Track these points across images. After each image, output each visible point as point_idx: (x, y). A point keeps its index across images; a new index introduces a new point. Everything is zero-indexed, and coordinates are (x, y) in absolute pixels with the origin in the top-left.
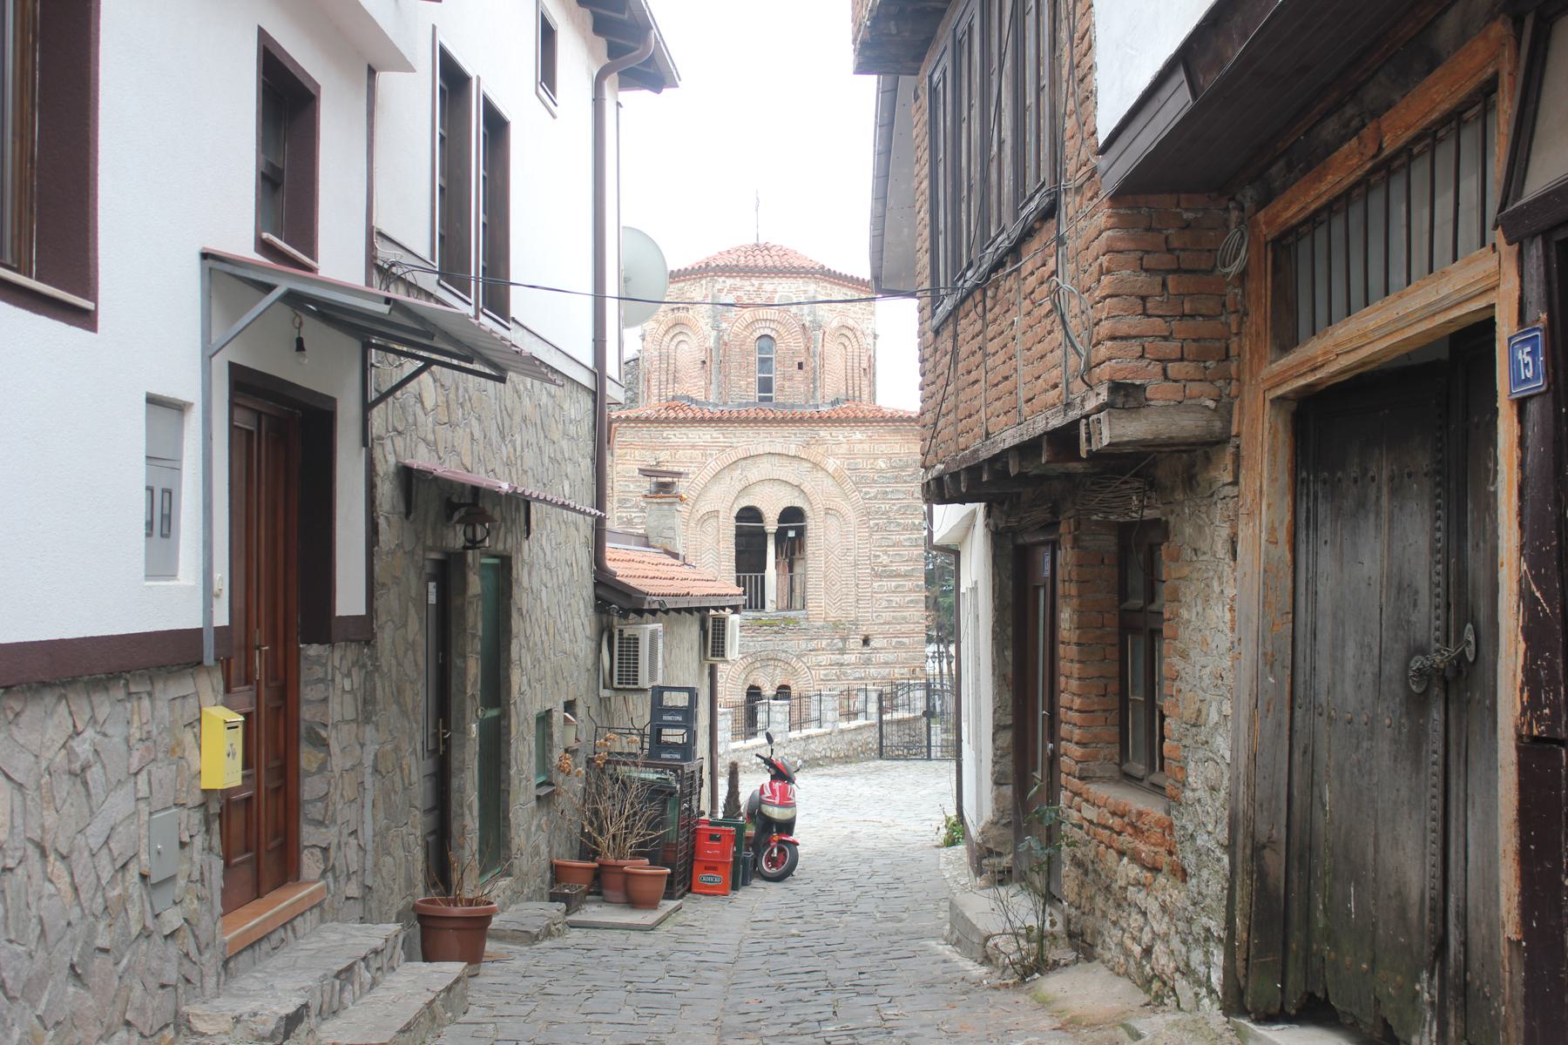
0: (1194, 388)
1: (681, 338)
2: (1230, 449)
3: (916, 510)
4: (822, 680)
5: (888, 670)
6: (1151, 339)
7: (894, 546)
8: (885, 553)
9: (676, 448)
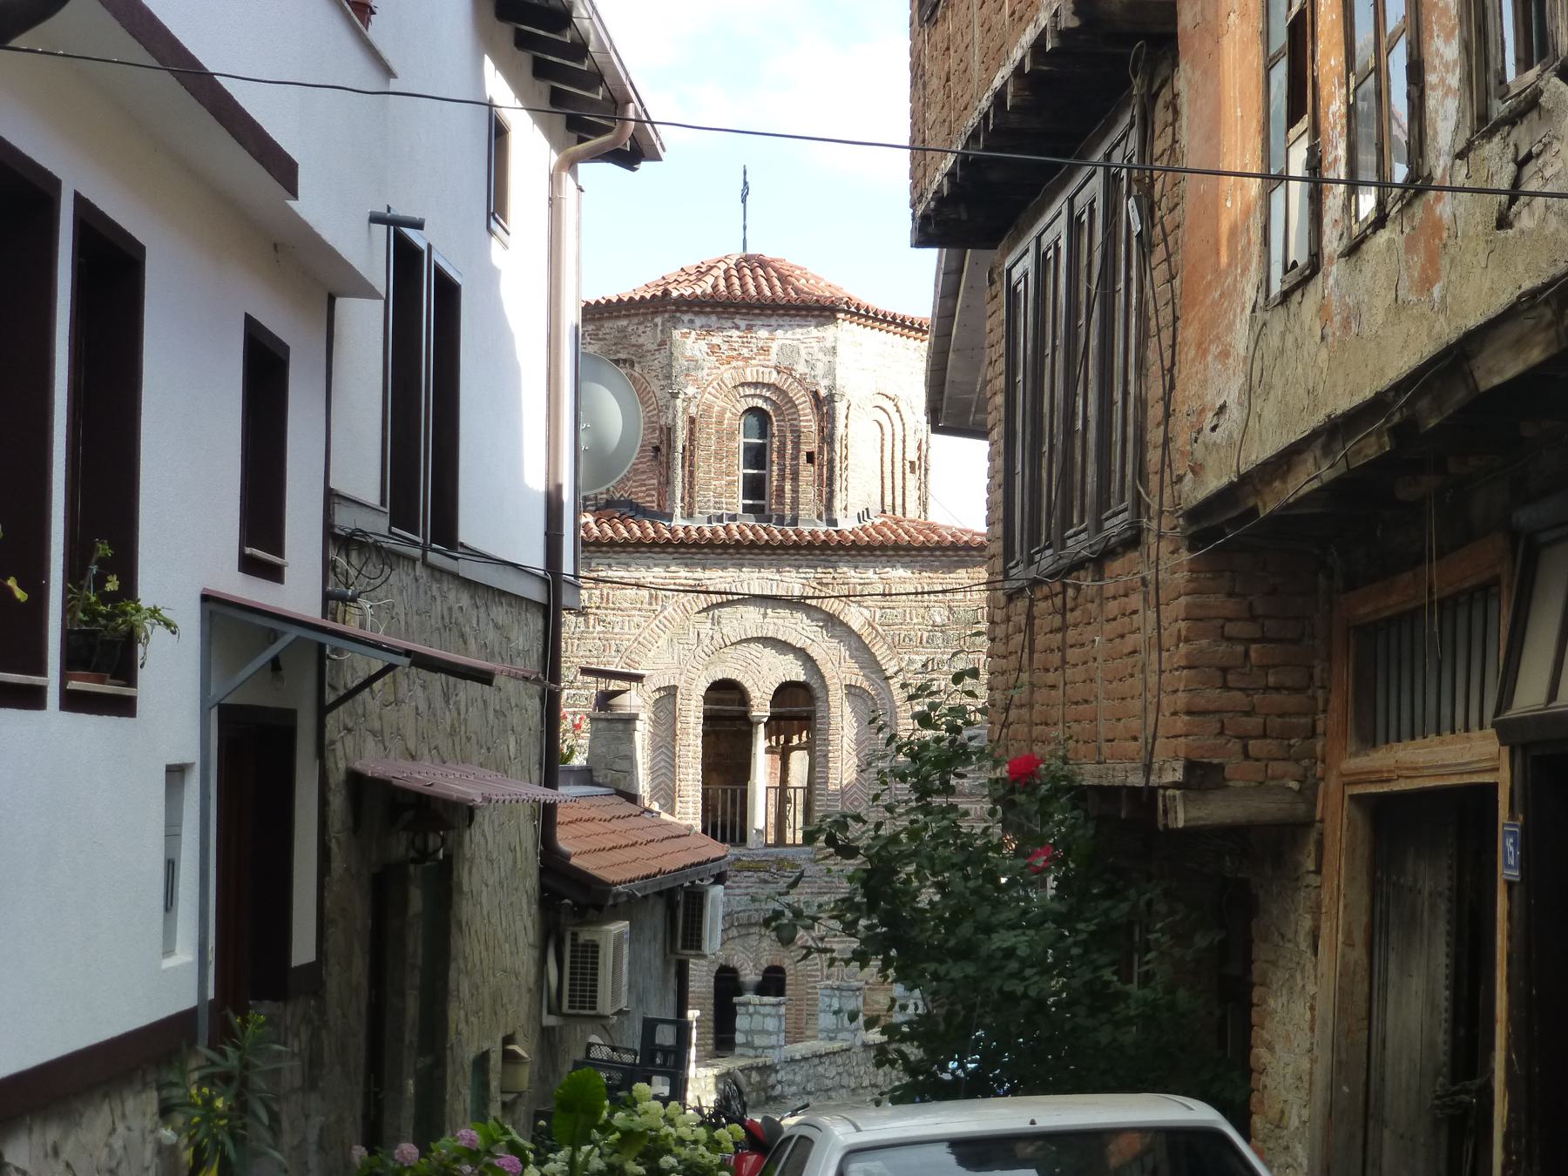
0: (1277, 768)
2: (1314, 836)
6: (1231, 715)
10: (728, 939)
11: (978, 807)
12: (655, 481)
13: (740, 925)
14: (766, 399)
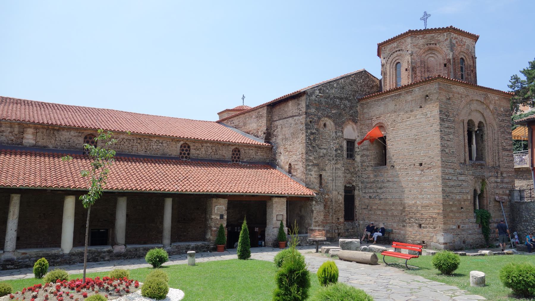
1: (431, 55)
5: (507, 185)
7: (506, 140)
12: (446, 72)
14: (464, 56)
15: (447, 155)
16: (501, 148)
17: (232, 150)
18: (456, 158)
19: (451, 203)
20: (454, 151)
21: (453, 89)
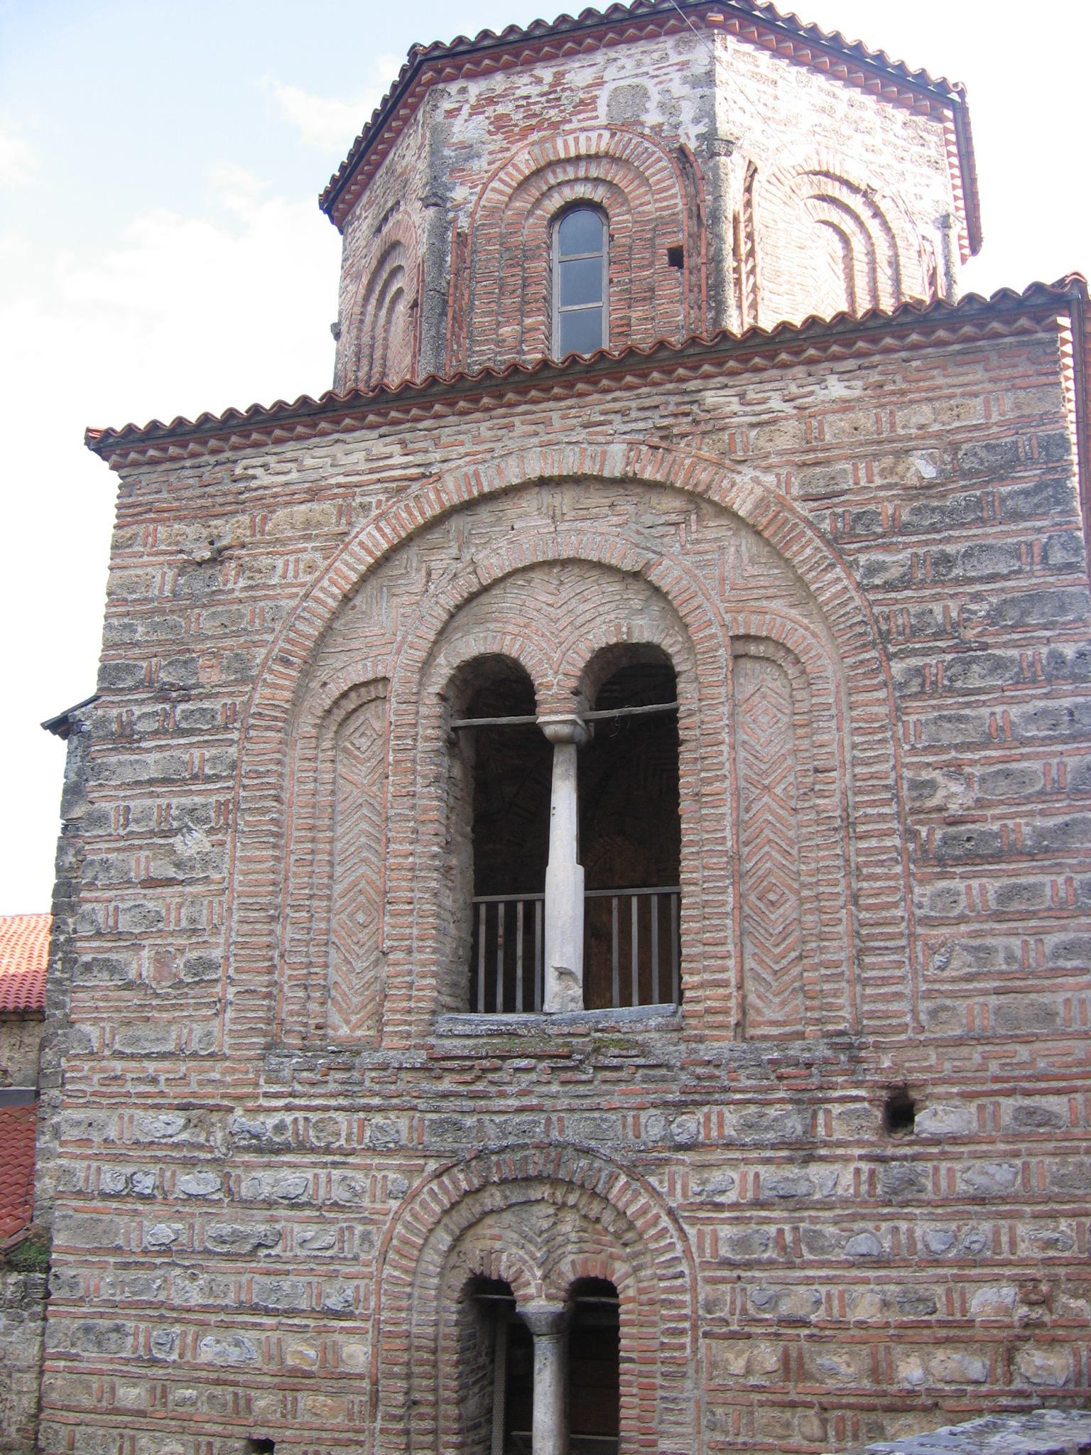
3: (1063, 609)
4: (729, 1264)
5: (986, 1226)
8: (955, 770)
9: (268, 503)
10: (485, 1214)
11: (1061, 880)
13: (504, 1181)
14: (597, 181)
15: (134, 998)
16: (897, 842)
17: (38, 1040)
18: (230, 1014)
19: (131, 1395)
20: (216, 954)
21: (266, 479)
